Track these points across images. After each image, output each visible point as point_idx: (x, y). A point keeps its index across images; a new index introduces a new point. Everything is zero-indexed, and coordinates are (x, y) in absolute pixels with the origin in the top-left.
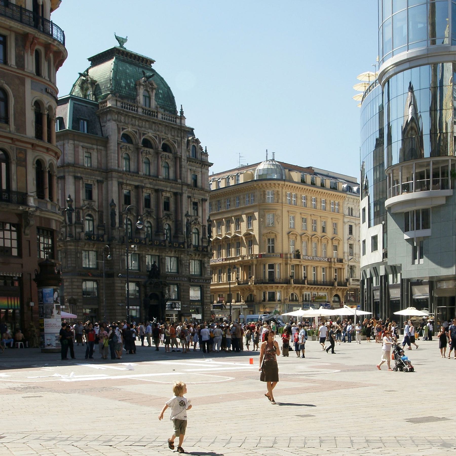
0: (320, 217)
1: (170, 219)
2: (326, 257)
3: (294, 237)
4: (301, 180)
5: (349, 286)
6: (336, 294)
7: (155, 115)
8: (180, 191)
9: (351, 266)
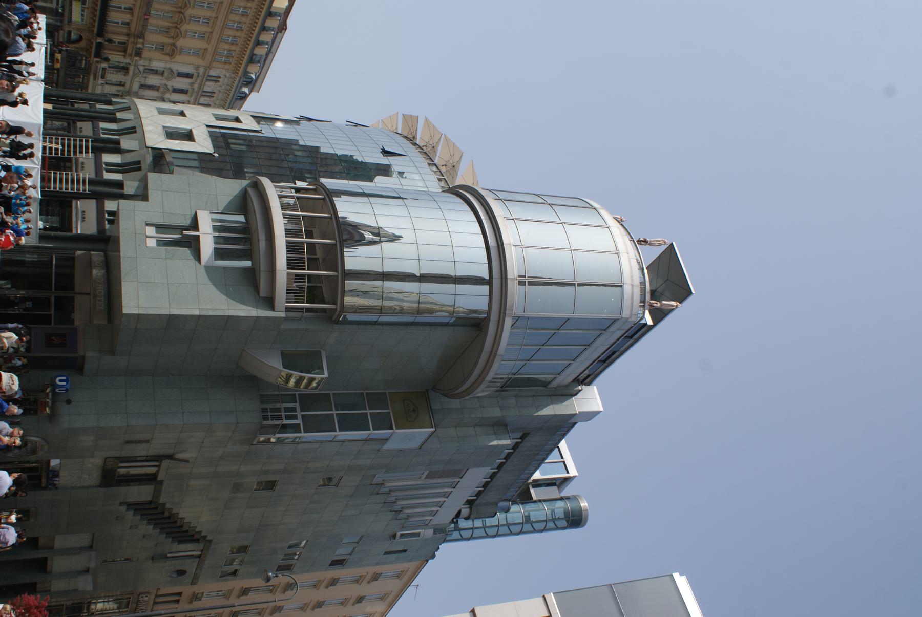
6: (83, 37)
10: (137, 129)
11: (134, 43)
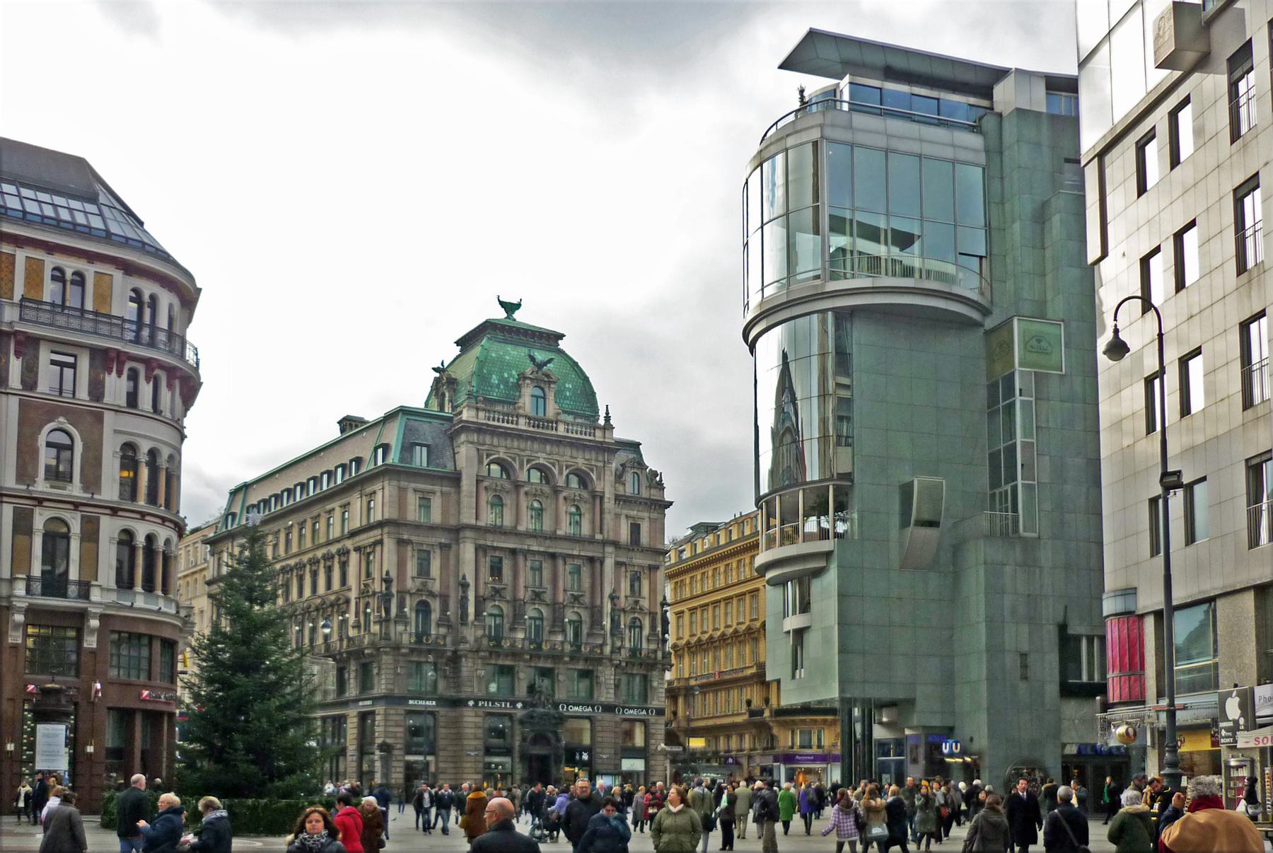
1: (579, 603)
7: (552, 427)
8: (600, 555)
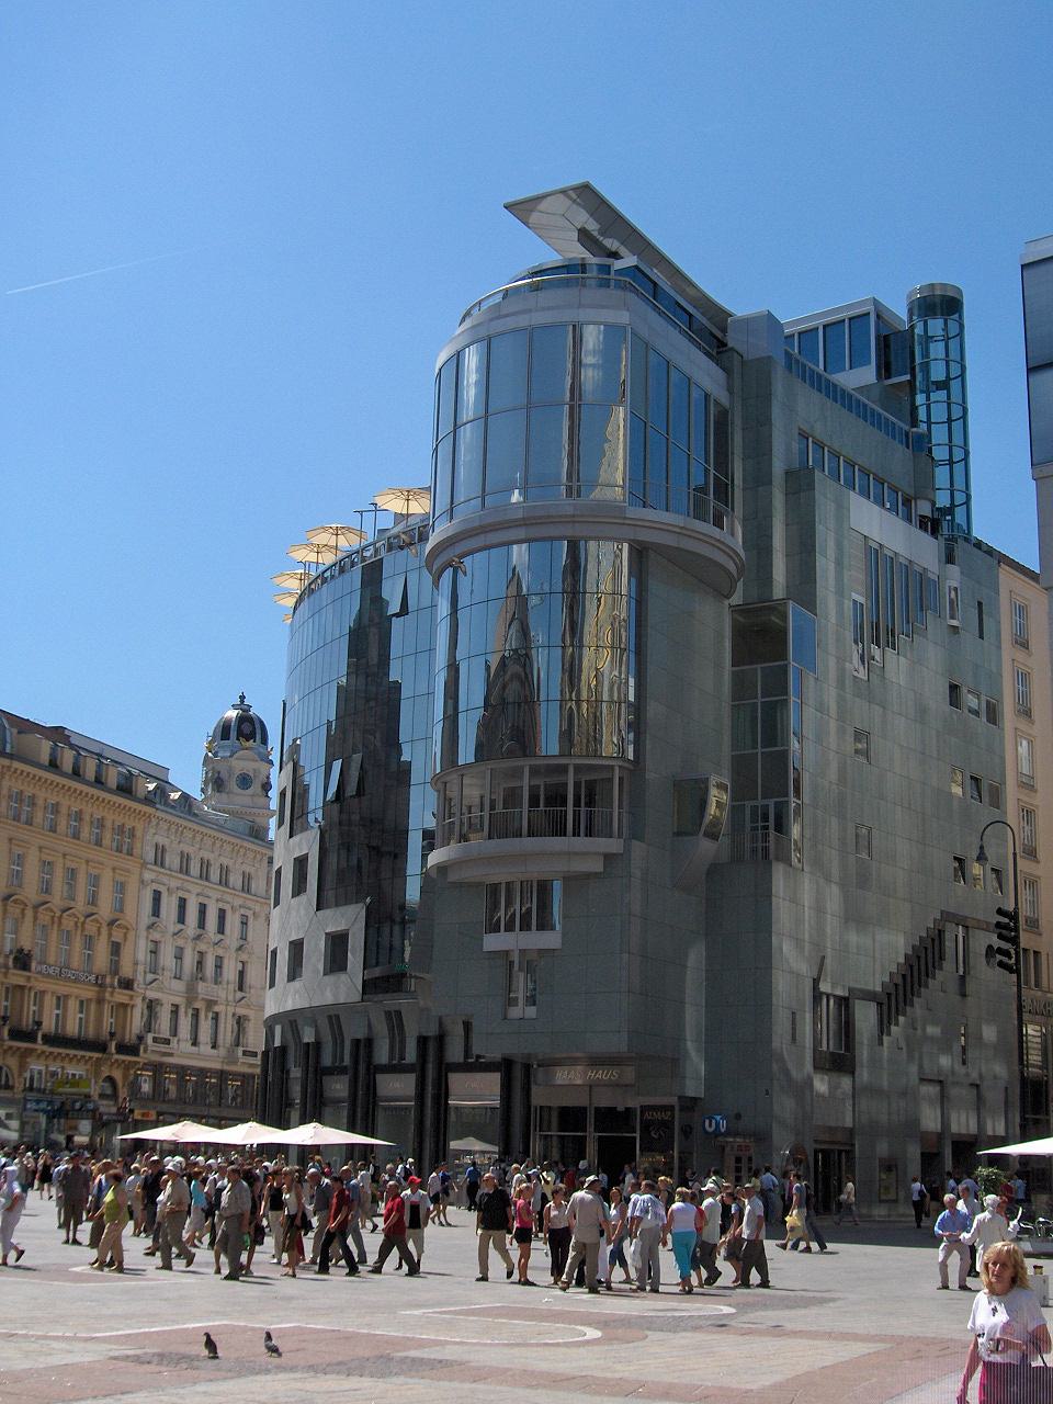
0: (87, 862)
2: (91, 973)
3: (18, 911)
4: (50, 761)
5: (146, 1056)
9: (151, 1001)
10: (332, 1013)
11: (112, 994)
